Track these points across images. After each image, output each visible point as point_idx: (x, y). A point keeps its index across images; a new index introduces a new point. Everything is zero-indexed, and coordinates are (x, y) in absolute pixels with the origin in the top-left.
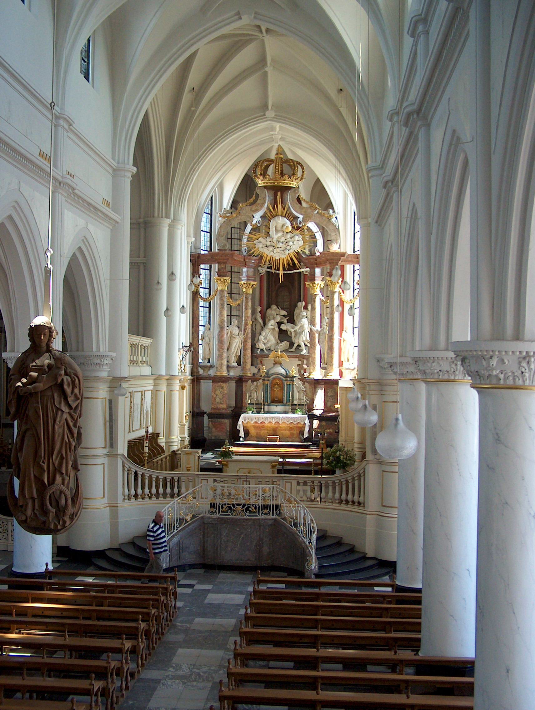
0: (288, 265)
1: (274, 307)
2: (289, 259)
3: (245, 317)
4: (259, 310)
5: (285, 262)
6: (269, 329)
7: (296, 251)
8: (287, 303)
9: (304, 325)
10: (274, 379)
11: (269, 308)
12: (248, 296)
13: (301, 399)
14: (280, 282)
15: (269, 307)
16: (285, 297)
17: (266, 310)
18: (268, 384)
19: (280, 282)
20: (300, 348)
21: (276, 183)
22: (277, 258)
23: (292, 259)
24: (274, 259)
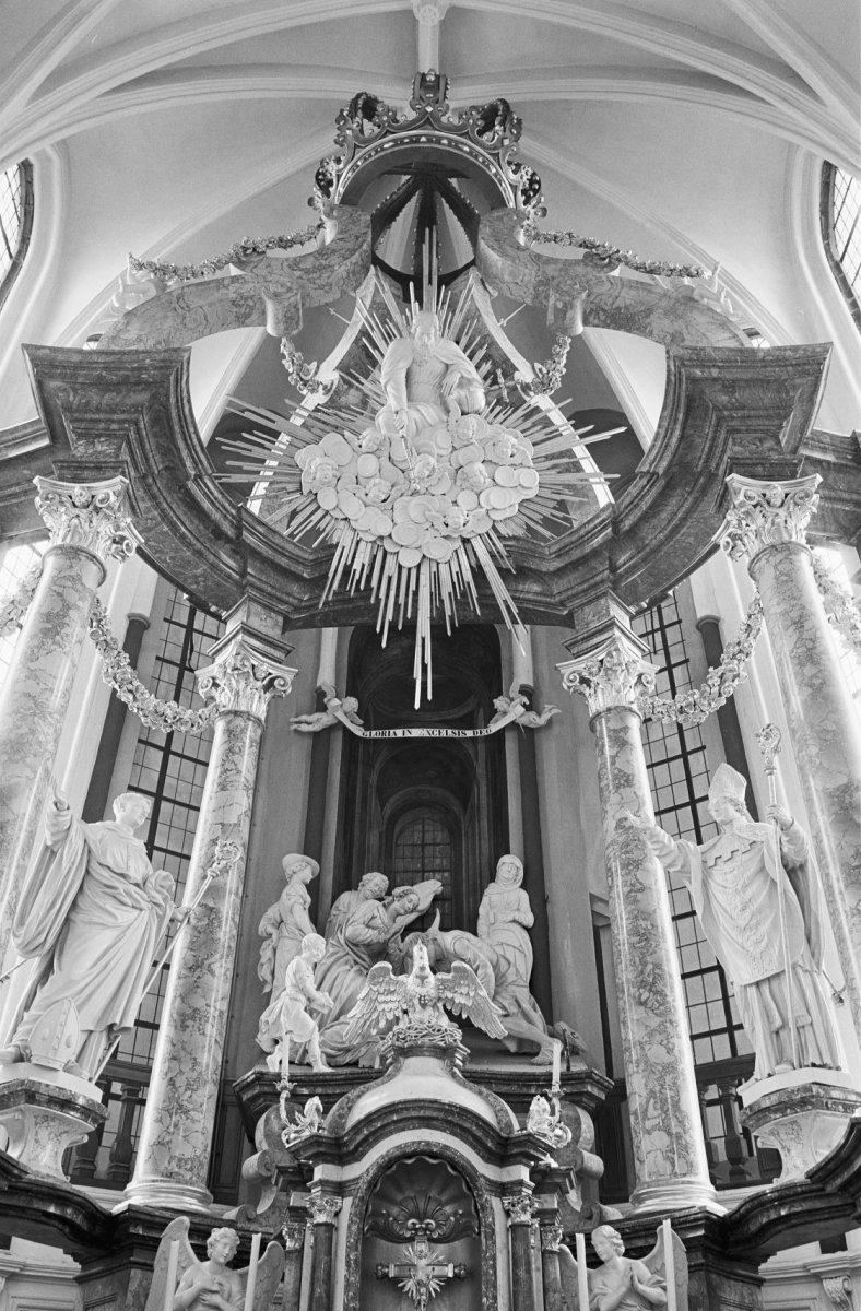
0: (461, 601)
1: (375, 881)
2: (468, 576)
5: (446, 589)
7: (504, 531)
11: (349, 889)
14: (417, 706)
16: (429, 850)
17: (335, 897)
18: (330, 1228)
19: (417, 706)
21: (423, 139)
22: (409, 559)
23: (478, 573)
24: (391, 569)
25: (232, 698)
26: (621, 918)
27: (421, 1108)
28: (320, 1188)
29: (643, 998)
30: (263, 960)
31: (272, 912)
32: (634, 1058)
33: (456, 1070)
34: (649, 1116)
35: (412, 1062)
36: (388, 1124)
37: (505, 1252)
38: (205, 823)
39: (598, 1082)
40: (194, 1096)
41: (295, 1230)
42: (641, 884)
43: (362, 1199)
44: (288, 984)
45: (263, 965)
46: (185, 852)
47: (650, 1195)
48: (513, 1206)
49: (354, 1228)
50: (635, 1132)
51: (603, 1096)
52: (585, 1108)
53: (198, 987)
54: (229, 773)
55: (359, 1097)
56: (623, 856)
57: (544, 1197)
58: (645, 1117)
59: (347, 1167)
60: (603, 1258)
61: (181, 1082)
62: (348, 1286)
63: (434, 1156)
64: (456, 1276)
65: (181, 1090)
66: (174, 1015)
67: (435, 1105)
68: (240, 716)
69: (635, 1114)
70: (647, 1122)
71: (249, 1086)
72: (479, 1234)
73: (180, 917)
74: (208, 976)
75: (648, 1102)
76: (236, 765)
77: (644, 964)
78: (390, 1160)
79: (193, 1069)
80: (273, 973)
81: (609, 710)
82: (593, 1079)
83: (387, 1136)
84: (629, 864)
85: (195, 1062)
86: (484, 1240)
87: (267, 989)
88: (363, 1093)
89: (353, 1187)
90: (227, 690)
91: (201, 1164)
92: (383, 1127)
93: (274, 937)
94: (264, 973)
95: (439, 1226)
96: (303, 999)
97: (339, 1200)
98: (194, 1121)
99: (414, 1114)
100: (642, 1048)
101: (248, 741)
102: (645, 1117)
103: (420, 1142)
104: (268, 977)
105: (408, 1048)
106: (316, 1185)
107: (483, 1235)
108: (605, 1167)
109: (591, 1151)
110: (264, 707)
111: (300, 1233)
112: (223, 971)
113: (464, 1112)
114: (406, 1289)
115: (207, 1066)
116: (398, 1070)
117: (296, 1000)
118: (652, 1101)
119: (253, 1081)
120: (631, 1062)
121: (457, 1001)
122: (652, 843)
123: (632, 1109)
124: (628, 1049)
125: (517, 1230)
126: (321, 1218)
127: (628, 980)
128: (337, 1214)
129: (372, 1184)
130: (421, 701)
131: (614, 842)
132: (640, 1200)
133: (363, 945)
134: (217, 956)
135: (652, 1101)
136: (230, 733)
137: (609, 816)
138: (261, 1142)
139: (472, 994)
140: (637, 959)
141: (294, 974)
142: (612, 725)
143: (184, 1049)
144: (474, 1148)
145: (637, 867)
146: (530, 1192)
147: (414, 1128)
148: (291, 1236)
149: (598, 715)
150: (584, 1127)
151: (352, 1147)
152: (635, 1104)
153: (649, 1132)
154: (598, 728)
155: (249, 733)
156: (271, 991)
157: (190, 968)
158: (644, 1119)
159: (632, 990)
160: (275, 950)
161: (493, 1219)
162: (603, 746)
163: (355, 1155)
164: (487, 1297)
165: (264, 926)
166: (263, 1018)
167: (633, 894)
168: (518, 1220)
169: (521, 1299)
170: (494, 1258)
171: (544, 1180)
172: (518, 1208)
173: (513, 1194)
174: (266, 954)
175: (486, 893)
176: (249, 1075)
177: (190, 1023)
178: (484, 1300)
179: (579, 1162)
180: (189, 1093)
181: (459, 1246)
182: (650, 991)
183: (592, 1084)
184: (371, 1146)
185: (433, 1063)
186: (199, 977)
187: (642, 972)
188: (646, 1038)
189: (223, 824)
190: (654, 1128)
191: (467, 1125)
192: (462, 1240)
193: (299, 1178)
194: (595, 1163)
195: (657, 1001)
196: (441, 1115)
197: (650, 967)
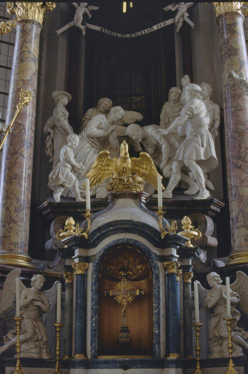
3: (16, 83)
4: (65, 101)
6: (91, 137)
8: (138, 98)
9: (198, 115)
10: (111, 251)
12: (29, 25)
13: (221, 338)
14: (125, 10)
15: (92, 103)
17: (85, 111)
18: (84, 277)
19: (125, 10)
20: (186, 192)
25: (25, 13)
26: (230, 124)
27: (124, 224)
28: (78, 259)
29: (239, 165)
30: (48, 146)
31: (49, 122)
32: (234, 193)
33: (142, 204)
34: (239, 221)
35: (121, 201)
36: (108, 231)
37: (164, 284)
38: (14, 80)
39: (216, 204)
40: (19, 215)
41: (69, 275)
42: (241, 107)
43: (97, 264)
44: (61, 159)
45: (47, 149)
46: (6, 92)
47: (238, 256)
48: (168, 266)
49: (94, 276)
50: (232, 228)
51: (219, 210)
52: (210, 216)
53: (16, 163)
54: (25, 53)
55: (95, 218)
56: (232, 92)
57: (185, 260)
58: (237, 221)
59: (91, 250)
60: (211, 286)
61: (12, 208)
62: (93, 300)
63: (130, 245)
64: (140, 294)
65: (13, 212)
66: (6, 177)
67: (131, 223)
68: (28, 22)
69: (233, 220)
70: (238, 224)
71: (45, 208)
72: (152, 278)
73: (5, 130)
74: (21, 158)
75: (238, 214)
76: (28, 49)
77: (240, 147)
78: (110, 247)
79: (17, 202)
80: (53, 152)
81: (226, 14)
82: (214, 203)
83: (108, 236)
84: (235, 96)
85: (18, 200)
86: (154, 281)
87: (51, 161)
88: (97, 216)
89: (93, 259)
90: (21, 9)
91: (25, 245)
92: (106, 232)
93: (52, 134)
94: (49, 152)
95: (134, 274)
96: (69, 166)
97: (87, 264)
98: (19, 226)
99: (120, 226)
100: (238, 189)
101: (34, 35)
102: (237, 221)
103: (123, 239)
104: (51, 154)
105: (118, 194)
106: (76, 258)
107: (154, 278)
108: (218, 243)
109: (212, 236)
110: (41, 16)
111: (71, 276)
112: (28, 155)
113: (145, 225)
114: (118, 300)
115: (24, 201)
116: (114, 205)
117: (66, 167)
118: (241, 214)
119: (47, 206)
120: (232, 195)
121: (141, 171)
122: (245, 88)
123: (231, 217)
124: (231, 189)
125: (170, 277)
126: (79, 272)
127: (232, 155)
128: (86, 270)
129: (102, 257)
130: (127, 10)
131: (227, 85)
132: (232, 258)
133: (97, 138)
134: (25, 147)
135: (241, 214)
136: (24, 32)
137: (225, 71)
138: (53, 234)
139: (149, 168)
140: (237, 145)
141: (65, 154)
142: (228, 22)
143: (12, 193)
144: (150, 241)
145: (239, 98)
146: (177, 260)
147: (121, 233)
148: (67, 277)
149: (221, 16)
150: (208, 225)
151: (92, 242)
152: (233, 215)
153: (238, 228)
154: (221, 23)
155: (34, 31)
156: (53, 162)
157: (12, 154)
158: (237, 222)
159: (234, 161)
160: (53, 141)
161: (159, 271)
162: (223, 33)
163: (94, 244)
164: (155, 303)
165: (47, 129)
166: (50, 176)
167: (236, 112)
168: (170, 271)
169: (171, 304)
170: (159, 288)
171: (185, 253)
172: (170, 267)
173: (168, 260)
174: (49, 143)
175: (163, 108)
176: (45, 204)
177: (14, 181)
178: (154, 304)
179: (205, 241)
180: (16, 214)
181: (143, 283)
182: (243, 161)
183: (213, 205)
184: (101, 241)
185: (130, 201)
186: (16, 159)
187: (239, 152)
188: (240, 184)
189: (23, 80)
190: (241, 226)
191: (146, 231)
192: (145, 280)
193: (69, 253)
194: (213, 241)
195: (246, 166)
196: (134, 227)
197: (243, 149)
